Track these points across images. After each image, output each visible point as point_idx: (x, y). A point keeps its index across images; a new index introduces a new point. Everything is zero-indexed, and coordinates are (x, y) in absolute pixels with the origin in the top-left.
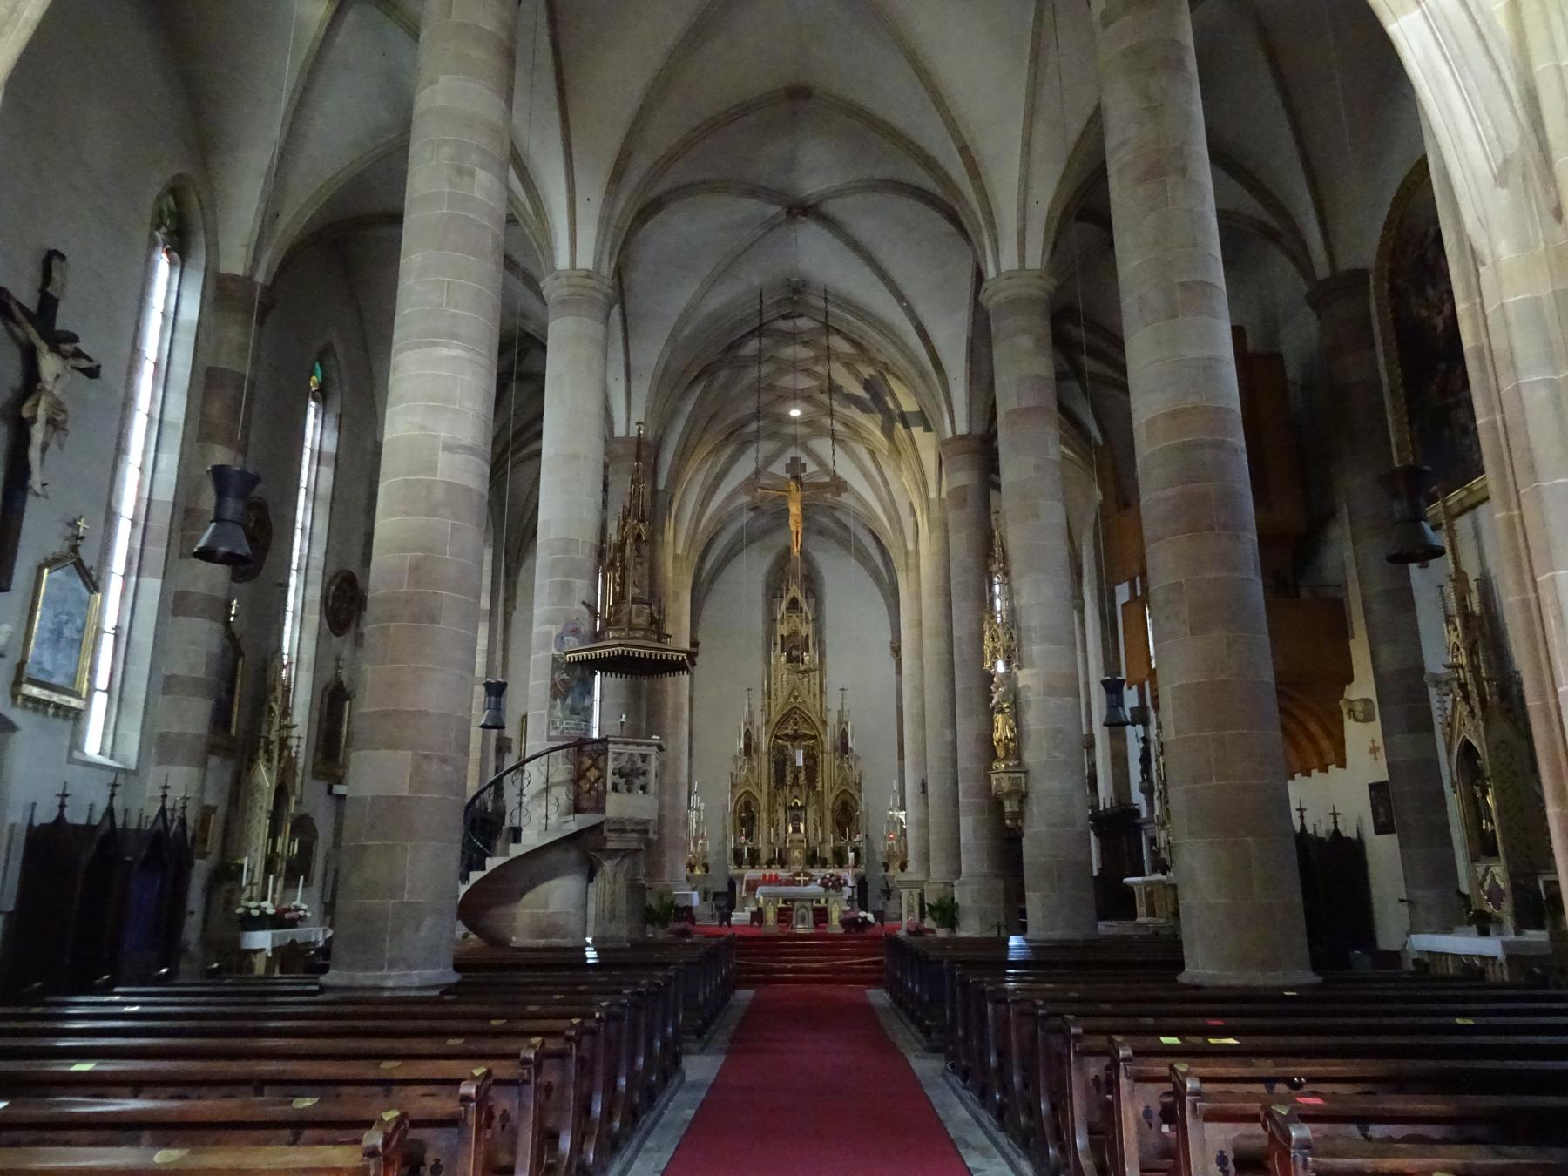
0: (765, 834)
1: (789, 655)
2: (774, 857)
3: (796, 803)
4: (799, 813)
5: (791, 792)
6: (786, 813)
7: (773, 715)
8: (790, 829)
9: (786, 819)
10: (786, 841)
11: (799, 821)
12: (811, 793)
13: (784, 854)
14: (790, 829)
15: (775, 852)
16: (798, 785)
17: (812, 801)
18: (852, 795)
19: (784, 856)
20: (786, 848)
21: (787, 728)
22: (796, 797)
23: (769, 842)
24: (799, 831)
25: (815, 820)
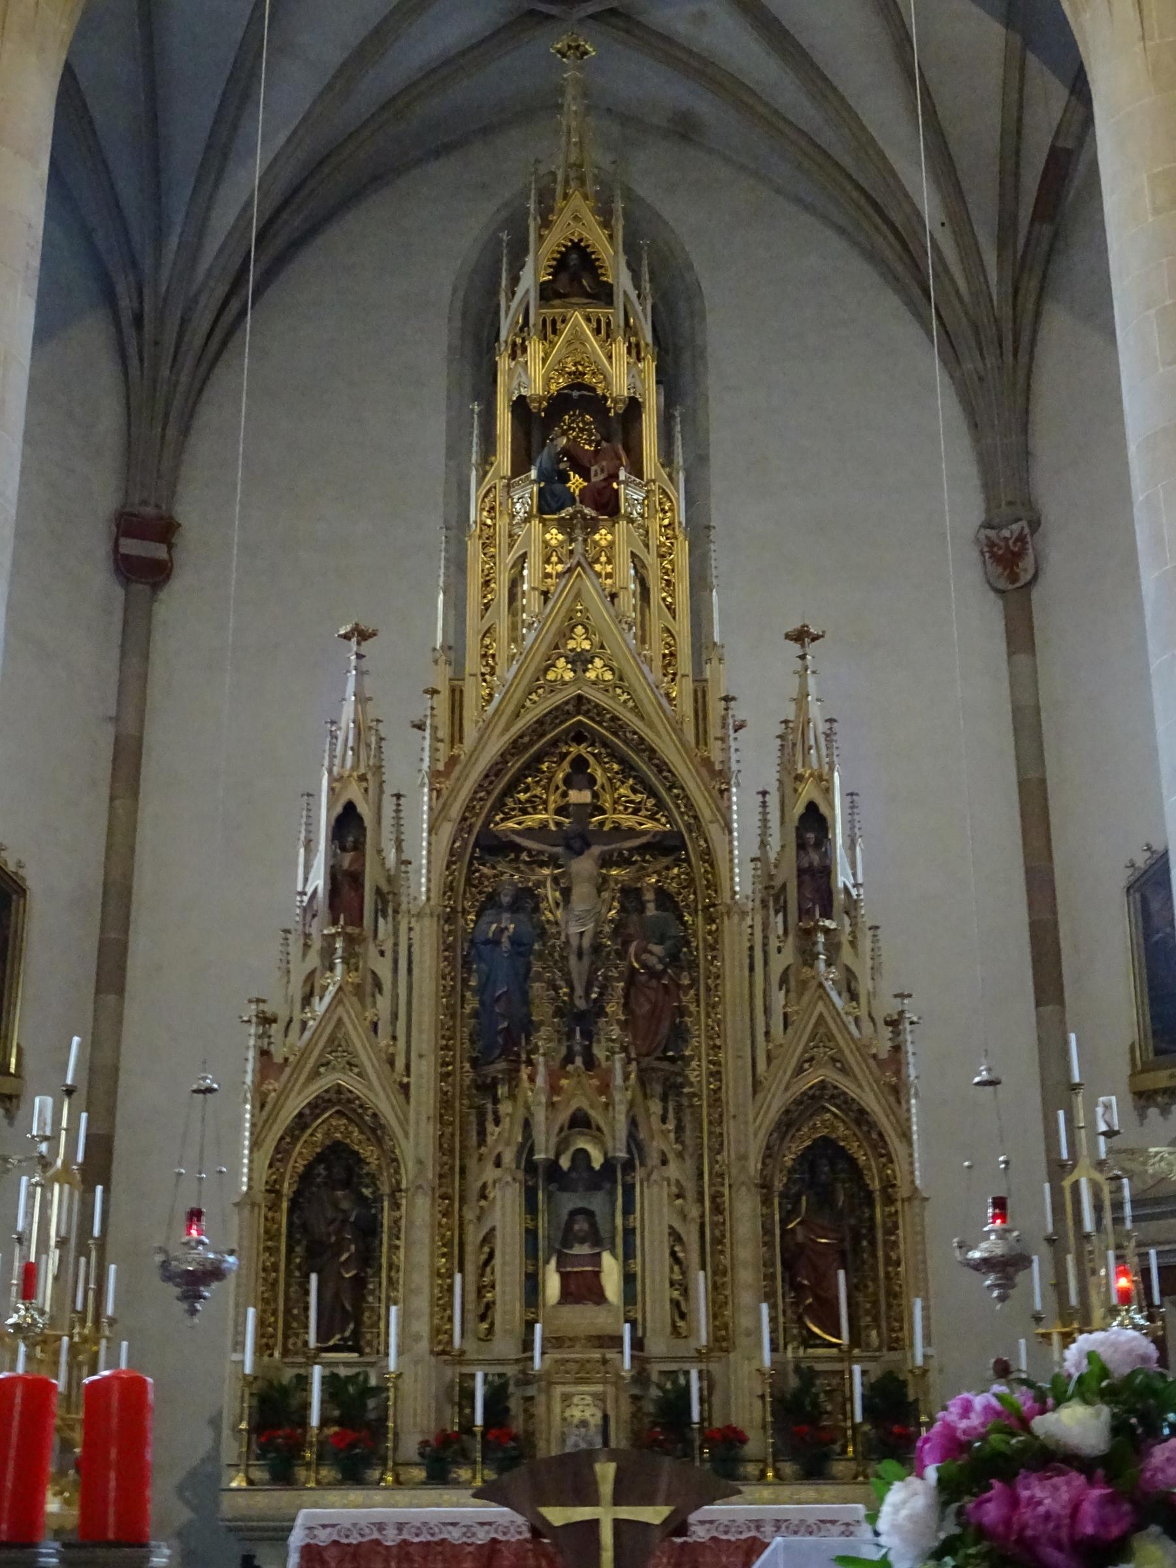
0: (422, 1303)
1: (553, 479)
2: (467, 1427)
3: (582, 1156)
4: (596, 1203)
5: (554, 1089)
6: (531, 1207)
7: (471, 732)
8: (552, 1285)
9: (531, 1235)
10: (528, 1345)
11: (596, 1239)
12: (656, 1107)
13: (514, 1405)
14: (552, 1285)
15: (468, 1396)
16: (590, 1063)
17: (659, 1141)
18: (861, 1117)
19: (517, 1425)
20: (526, 1379)
21: (532, 805)
22: (580, 1122)
23: (443, 1351)
24: (598, 1297)
25: (676, 1236)
